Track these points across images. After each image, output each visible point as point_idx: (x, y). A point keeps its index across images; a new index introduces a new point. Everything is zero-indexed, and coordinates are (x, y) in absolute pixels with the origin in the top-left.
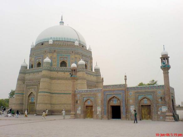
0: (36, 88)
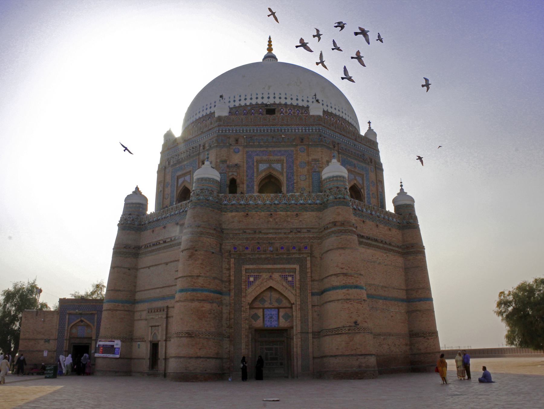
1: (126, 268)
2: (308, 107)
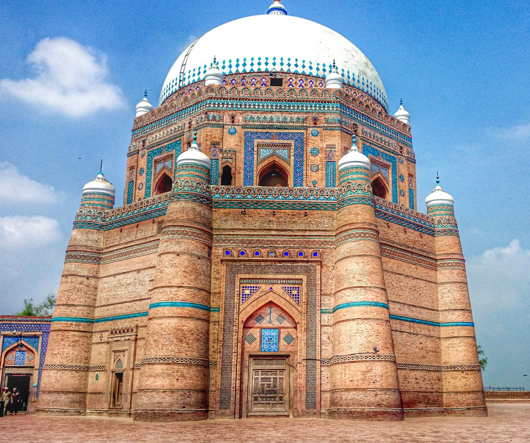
0: (304, 283)
1: (84, 276)
2: (324, 78)
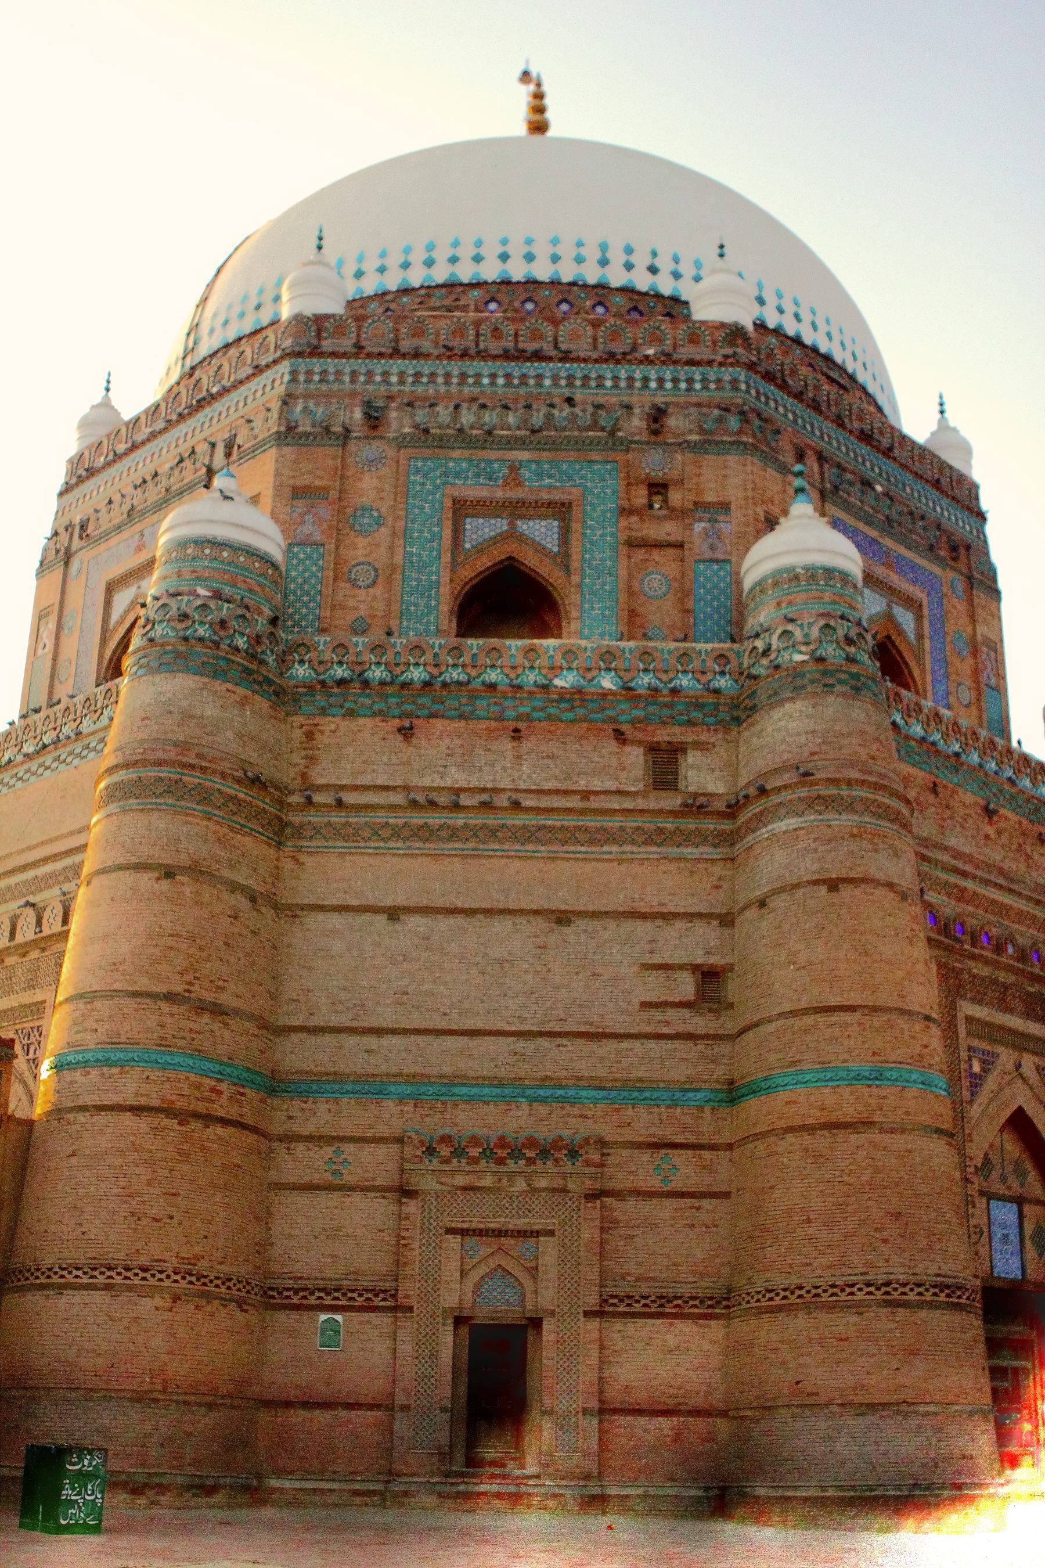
1: (243, 889)
